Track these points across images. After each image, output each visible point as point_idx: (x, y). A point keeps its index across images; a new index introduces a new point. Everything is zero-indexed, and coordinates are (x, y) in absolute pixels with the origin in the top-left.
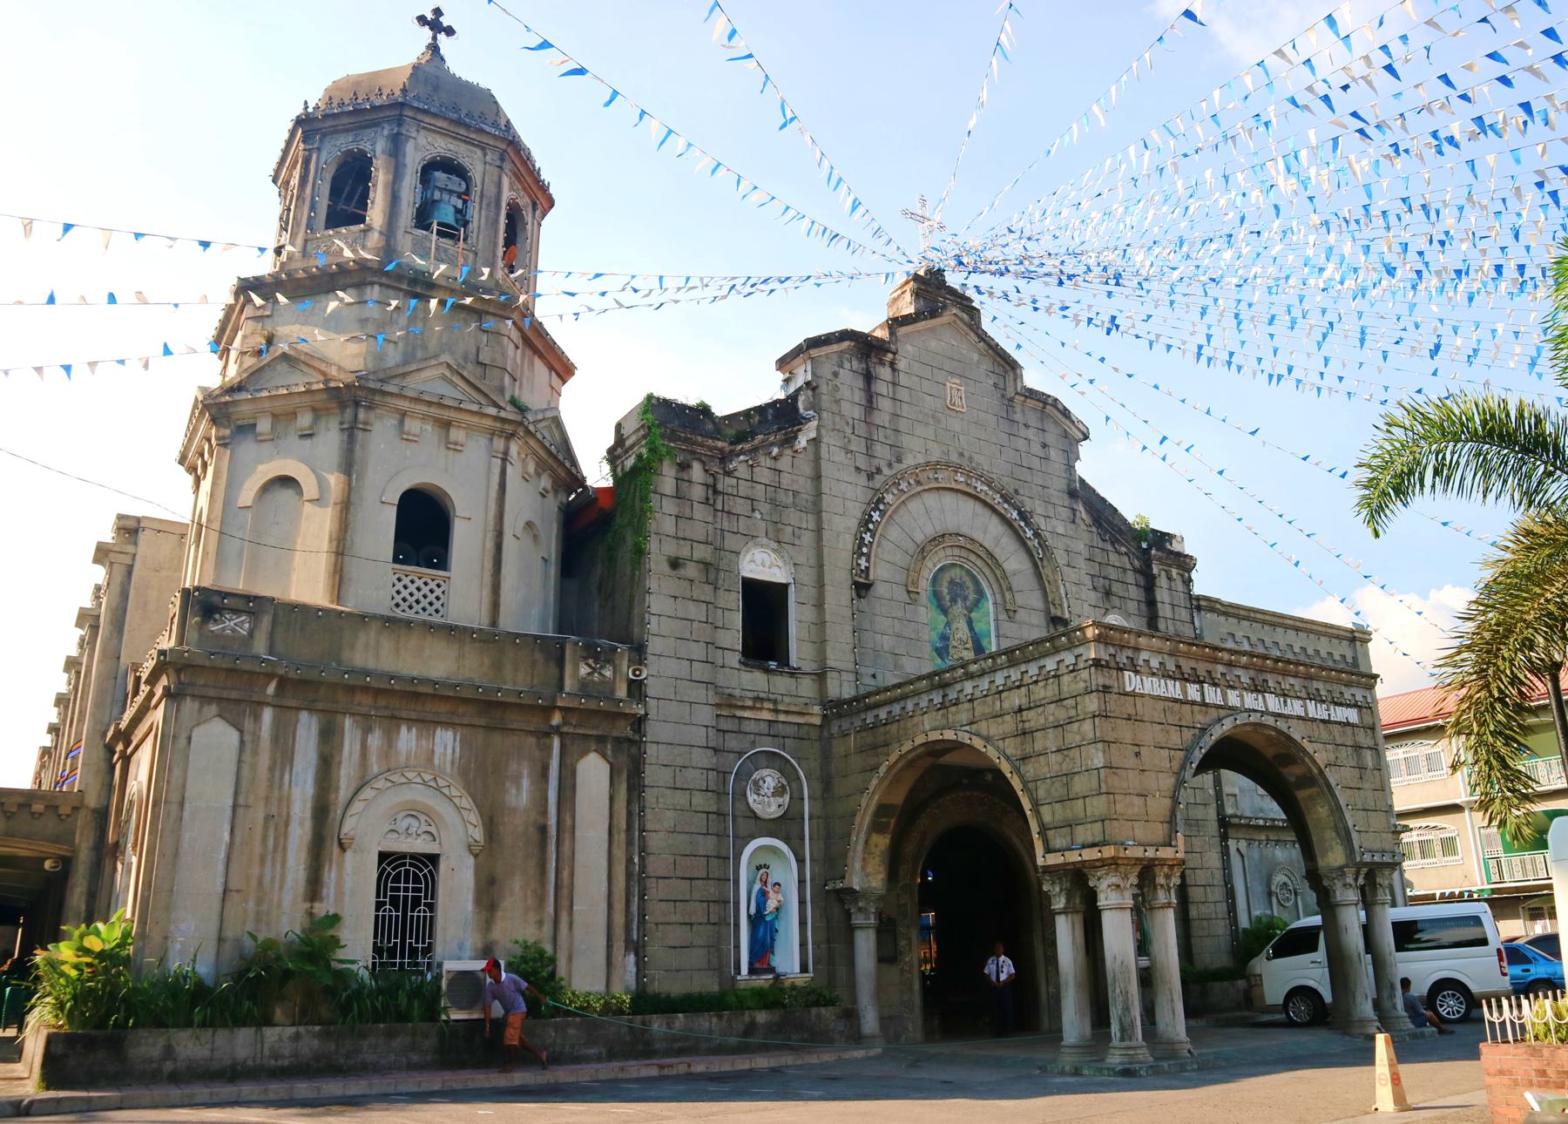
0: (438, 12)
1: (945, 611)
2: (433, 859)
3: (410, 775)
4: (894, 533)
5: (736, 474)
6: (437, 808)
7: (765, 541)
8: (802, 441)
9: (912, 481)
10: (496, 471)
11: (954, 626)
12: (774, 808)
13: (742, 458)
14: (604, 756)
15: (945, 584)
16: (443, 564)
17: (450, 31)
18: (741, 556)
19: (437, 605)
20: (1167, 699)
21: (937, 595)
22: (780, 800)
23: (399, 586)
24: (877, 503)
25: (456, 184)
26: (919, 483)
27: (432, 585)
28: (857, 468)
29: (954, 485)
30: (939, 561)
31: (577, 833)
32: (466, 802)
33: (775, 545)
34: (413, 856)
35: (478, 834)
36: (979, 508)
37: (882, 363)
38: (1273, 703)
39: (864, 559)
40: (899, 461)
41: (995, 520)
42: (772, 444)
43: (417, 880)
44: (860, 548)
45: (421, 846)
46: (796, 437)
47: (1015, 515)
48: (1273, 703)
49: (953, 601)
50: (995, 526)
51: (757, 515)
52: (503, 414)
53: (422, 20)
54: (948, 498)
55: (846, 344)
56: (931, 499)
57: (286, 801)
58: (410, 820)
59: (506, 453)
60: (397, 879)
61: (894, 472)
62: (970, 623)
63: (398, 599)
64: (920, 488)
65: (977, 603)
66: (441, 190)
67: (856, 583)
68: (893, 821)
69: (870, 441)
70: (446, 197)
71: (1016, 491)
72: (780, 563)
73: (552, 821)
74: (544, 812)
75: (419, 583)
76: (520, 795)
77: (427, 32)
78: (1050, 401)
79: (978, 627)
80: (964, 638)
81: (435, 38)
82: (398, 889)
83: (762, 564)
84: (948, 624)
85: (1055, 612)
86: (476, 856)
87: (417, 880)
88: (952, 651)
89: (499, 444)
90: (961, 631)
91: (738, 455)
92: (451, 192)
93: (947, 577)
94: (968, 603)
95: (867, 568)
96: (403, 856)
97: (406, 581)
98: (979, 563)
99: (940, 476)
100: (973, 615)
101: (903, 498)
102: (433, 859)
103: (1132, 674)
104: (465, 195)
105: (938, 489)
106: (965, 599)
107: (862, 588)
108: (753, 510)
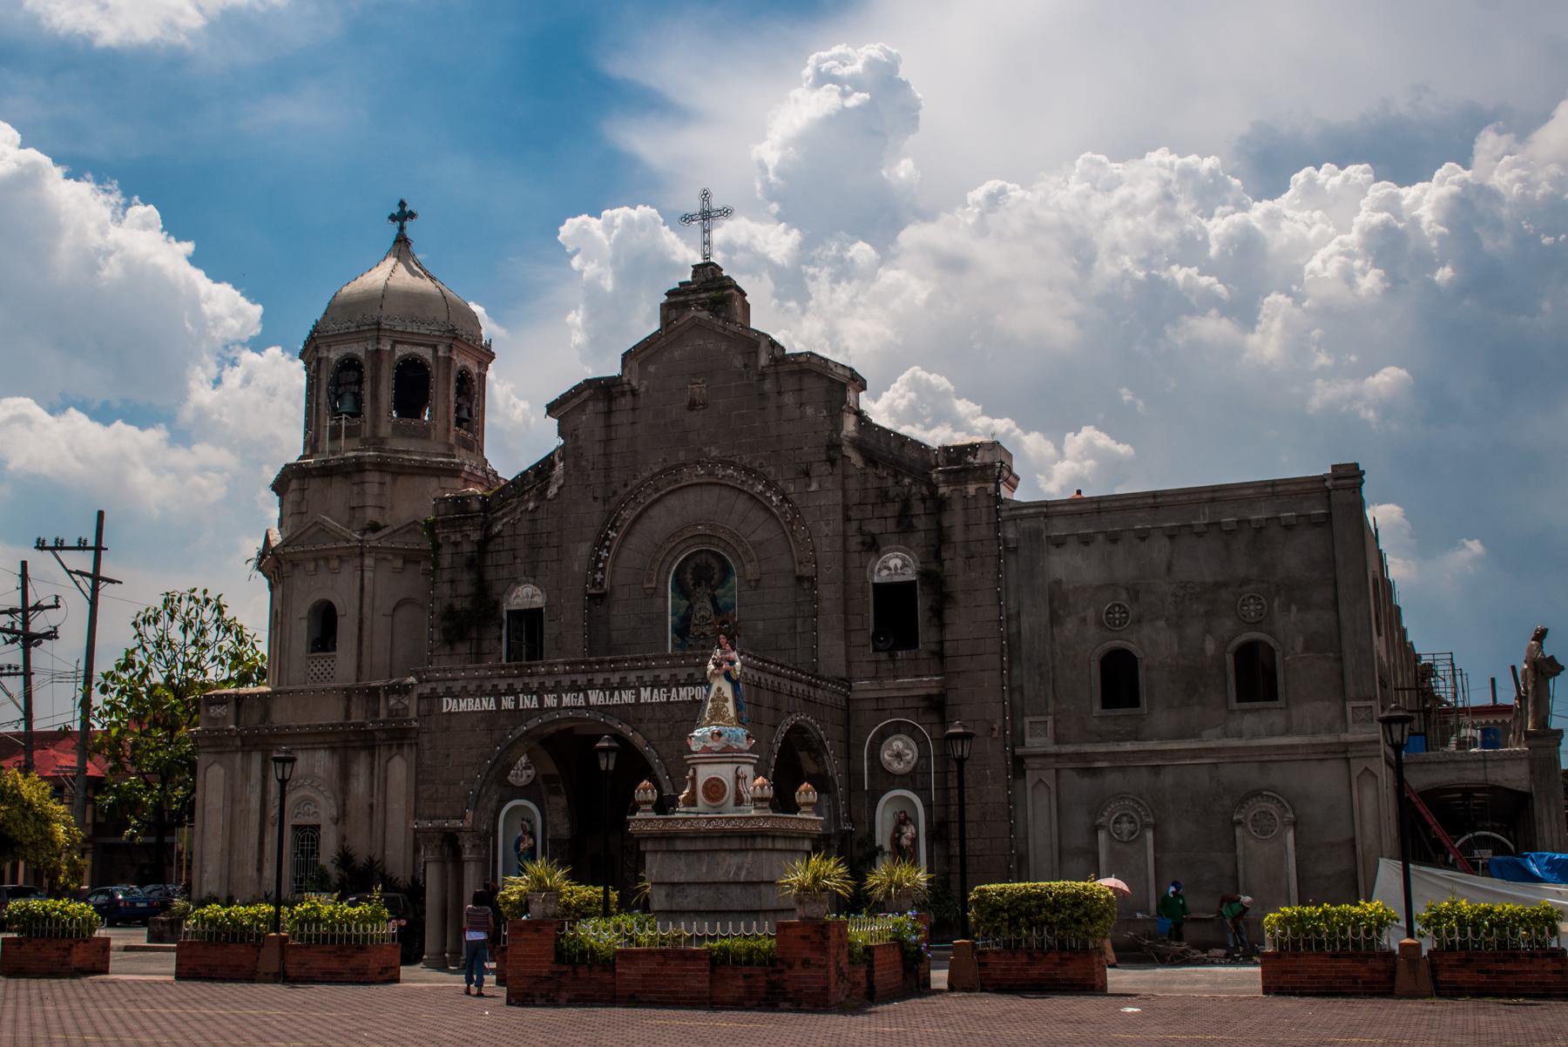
0: (402, 204)
1: (687, 597)
2: (319, 826)
3: (301, 781)
4: (634, 541)
5: (503, 534)
6: (317, 798)
7: (524, 578)
8: (553, 490)
9: (649, 491)
10: (358, 579)
11: (697, 607)
12: (524, 778)
13: (505, 520)
14: (402, 756)
15: (689, 571)
16: (334, 649)
17: (412, 215)
18: (505, 596)
19: (332, 674)
20: (481, 712)
21: (680, 587)
22: (529, 771)
23: (312, 667)
24: (611, 520)
25: (352, 375)
26: (657, 490)
27: (329, 662)
28: (595, 499)
29: (695, 480)
30: (681, 552)
31: (388, 807)
32: (326, 794)
33: (532, 580)
34: (311, 826)
35: (334, 812)
36: (726, 493)
37: (623, 394)
38: (595, 697)
39: (600, 573)
40: (635, 477)
41: (743, 497)
42: (528, 501)
43: (313, 840)
44: (597, 564)
45: (311, 821)
46: (547, 489)
47: (760, 487)
48: (595, 697)
49: (697, 584)
50: (741, 504)
51: (519, 561)
52: (351, 544)
53: (393, 218)
54: (691, 495)
55: (586, 394)
56: (672, 501)
57: (248, 801)
58: (306, 808)
59: (362, 565)
60: (303, 840)
61: (629, 488)
62: (714, 600)
63: (312, 674)
64: (658, 495)
65: (724, 580)
66: (345, 384)
67: (589, 595)
68: (561, 785)
69: (608, 469)
70: (348, 387)
71: (761, 465)
72: (539, 592)
73: (375, 802)
74: (372, 796)
75: (322, 662)
76: (359, 786)
77: (398, 224)
78: (802, 359)
79: (721, 603)
80: (707, 615)
81: (402, 228)
82: (303, 845)
83: (525, 596)
84: (691, 607)
85: (799, 570)
86: (336, 823)
87: (313, 840)
88: (692, 629)
89: (357, 562)
90: (704, 608)
91: (502, 519)
92: (351, 383)
93: (692, 564)
94: (713, 582)
95: (602, 579)
96: (306, 826)
97: (316, 662)
98: (721, 544)
99: (679, 477)
100: (719, 592)
101: (639, 510)
102: (319, 826)
103: (450, 700)
104: (359, 382)
105: (680, 488)
106: (711, 578)
107: (598, 599)
108: (515, 558)
